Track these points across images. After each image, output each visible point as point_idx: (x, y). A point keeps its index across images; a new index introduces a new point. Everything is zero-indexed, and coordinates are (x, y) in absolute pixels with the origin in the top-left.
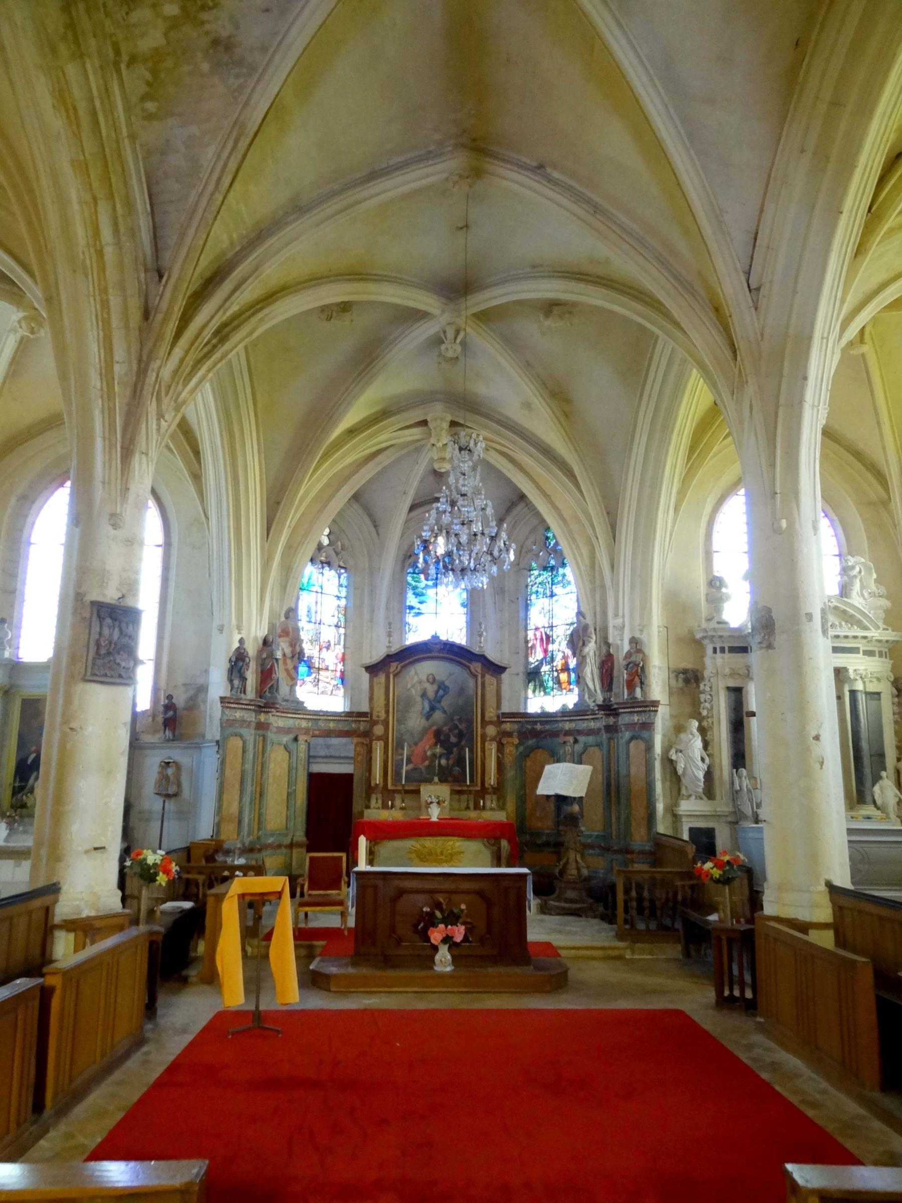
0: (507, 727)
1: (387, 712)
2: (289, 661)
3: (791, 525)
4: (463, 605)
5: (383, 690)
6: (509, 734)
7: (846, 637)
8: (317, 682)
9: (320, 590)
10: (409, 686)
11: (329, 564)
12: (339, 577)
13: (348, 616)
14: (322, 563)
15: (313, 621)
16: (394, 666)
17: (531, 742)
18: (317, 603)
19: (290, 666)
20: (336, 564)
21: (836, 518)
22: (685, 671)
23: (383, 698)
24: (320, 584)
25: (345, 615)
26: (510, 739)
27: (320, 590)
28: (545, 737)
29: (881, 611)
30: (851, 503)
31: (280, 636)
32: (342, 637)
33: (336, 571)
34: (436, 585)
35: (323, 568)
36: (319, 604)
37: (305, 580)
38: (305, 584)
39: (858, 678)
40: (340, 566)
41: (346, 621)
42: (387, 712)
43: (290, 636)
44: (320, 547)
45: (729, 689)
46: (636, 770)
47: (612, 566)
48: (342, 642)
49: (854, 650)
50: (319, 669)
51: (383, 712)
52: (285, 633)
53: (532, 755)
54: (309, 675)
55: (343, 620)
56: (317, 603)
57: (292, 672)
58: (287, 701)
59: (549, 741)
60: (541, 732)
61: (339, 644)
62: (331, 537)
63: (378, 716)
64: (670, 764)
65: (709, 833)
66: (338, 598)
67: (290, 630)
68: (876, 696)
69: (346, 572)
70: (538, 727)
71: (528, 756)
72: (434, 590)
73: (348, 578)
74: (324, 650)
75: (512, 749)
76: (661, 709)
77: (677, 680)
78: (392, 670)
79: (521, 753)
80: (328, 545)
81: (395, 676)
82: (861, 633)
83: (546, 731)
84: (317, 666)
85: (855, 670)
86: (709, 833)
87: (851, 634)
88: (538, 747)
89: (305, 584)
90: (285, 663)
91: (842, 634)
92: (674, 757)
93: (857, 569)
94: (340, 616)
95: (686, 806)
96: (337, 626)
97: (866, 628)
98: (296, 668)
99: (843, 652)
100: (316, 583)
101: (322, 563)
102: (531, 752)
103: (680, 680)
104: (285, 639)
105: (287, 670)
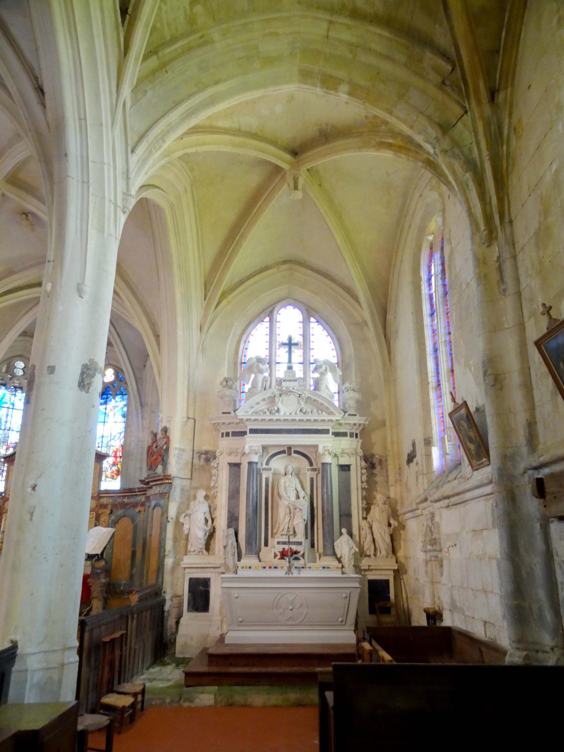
0: (104, 501)
3: (53, 287)
4: (124, 416)
6: (104, 506)
7: (315, 421)
11: (21, 388)
14: (15, 387)
17: (120, 512)
18: (7, 415)
21: (334, 336)
22: (206, 453)
24: (12, 401)
26: (104, 510)
27: (11, 407)
28: (130, 507)
29: (354, 402)
30: (343, 324)
34: (106, 403)
35: (16, 391)
36: (9, 418)
39: (326, 453)
44: (14, 376)
45: (230, 465)
46: (155, 532)
47: (160, 376)
49: (326, 431)
53: (120, 521)
56: (7, 415)
59: (131, 511)
60: (127, 504)
64: (179, 525)
65: (206, 583)
68: (346, 468)
70: (126, 500)
71: (117, 522)
72: (104, 406)
75: (106, 518)
76: (177, 483)
77: (199, 460)
79: (113, 521)
80: (22, 376)
82: (327, 418)
83: (130, 504)
85: (324, 447)
86: (206, 583)
87: (319, 418)
88: (125, 516)
91: (313, 418)
92: (181, 520)
93: (324, 368)
95: (187, 560)
97: (332, 413)
99: (316, 433)
100: (8, 401)
101: (15, 387)
102: (120, 519)
103: (202, 460)
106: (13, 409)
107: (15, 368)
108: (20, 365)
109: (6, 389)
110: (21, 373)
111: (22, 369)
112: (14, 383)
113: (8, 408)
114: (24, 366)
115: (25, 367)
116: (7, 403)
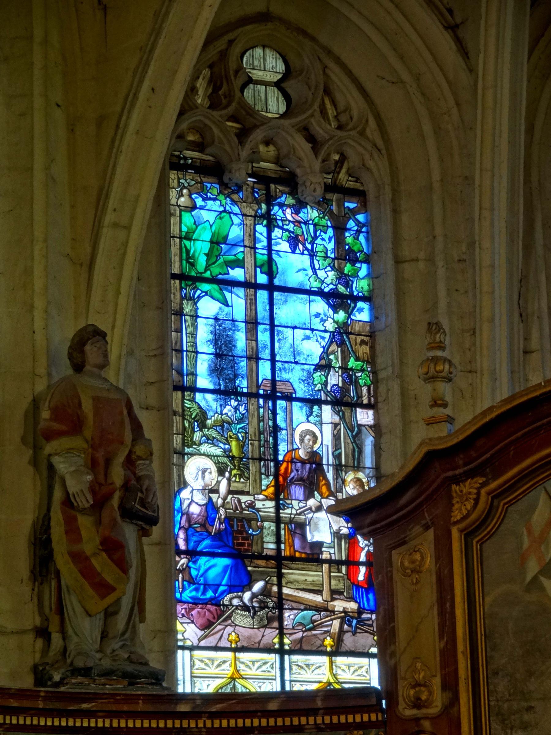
1: (450, 684)
2: (85, 522)
5: (429, 593)
8: (272, 610)
9: (262, 279)
10: (533, 568)
11: (291, 182)
12: (340, 229)
13: (380, 360)
14: (263, 179)
15: (243, 384)
16: (467, 499)
19: (90, 543)
20: (314, 181)
23: (431, 623)
25: (371, 360)
27: (262, 279)
31: (49, 435)
32: (368, 442)
33: (322, 204)
35: (270, 200)
37: (200, 248)
38: (202, 262)
40: (330, 188)
41: (375, 381)
42: (450, 684)
43: (88, 432)
44: (247, 122)
48: (368, 461)
50: (279, 561)
51: (437, 682)
52: (69, 420)
54: (241, 582)
55: (364, 379)
57: (101, 563)
58: (86, 672)
61: (358, 467)
62: (291, 86)
63: (417, 704)
66: (338, 300)
67: (87, 407)
69: (364, 207)
73: (369, 229)
74: (298, 491)
78: (457, 515)
80: (283, 116)
81: (469, 535)
84: (270, 546)
89: (202, 262)
90: (72, 530)
94: (352, 363)
96: (342, 402)
98: (113, 547)
101: (263, 179)
104: (65, 442)
105: (79, 559)
106: (271, 288)
107: (250, 81)
108: (266, 65)
109: (228, 188)
110: (275, 104)
111: (278, 84)
112: (255, 157)
113: (246, 285)
114: (281, 67)
115: (287, 75)
116: (238, 264)
